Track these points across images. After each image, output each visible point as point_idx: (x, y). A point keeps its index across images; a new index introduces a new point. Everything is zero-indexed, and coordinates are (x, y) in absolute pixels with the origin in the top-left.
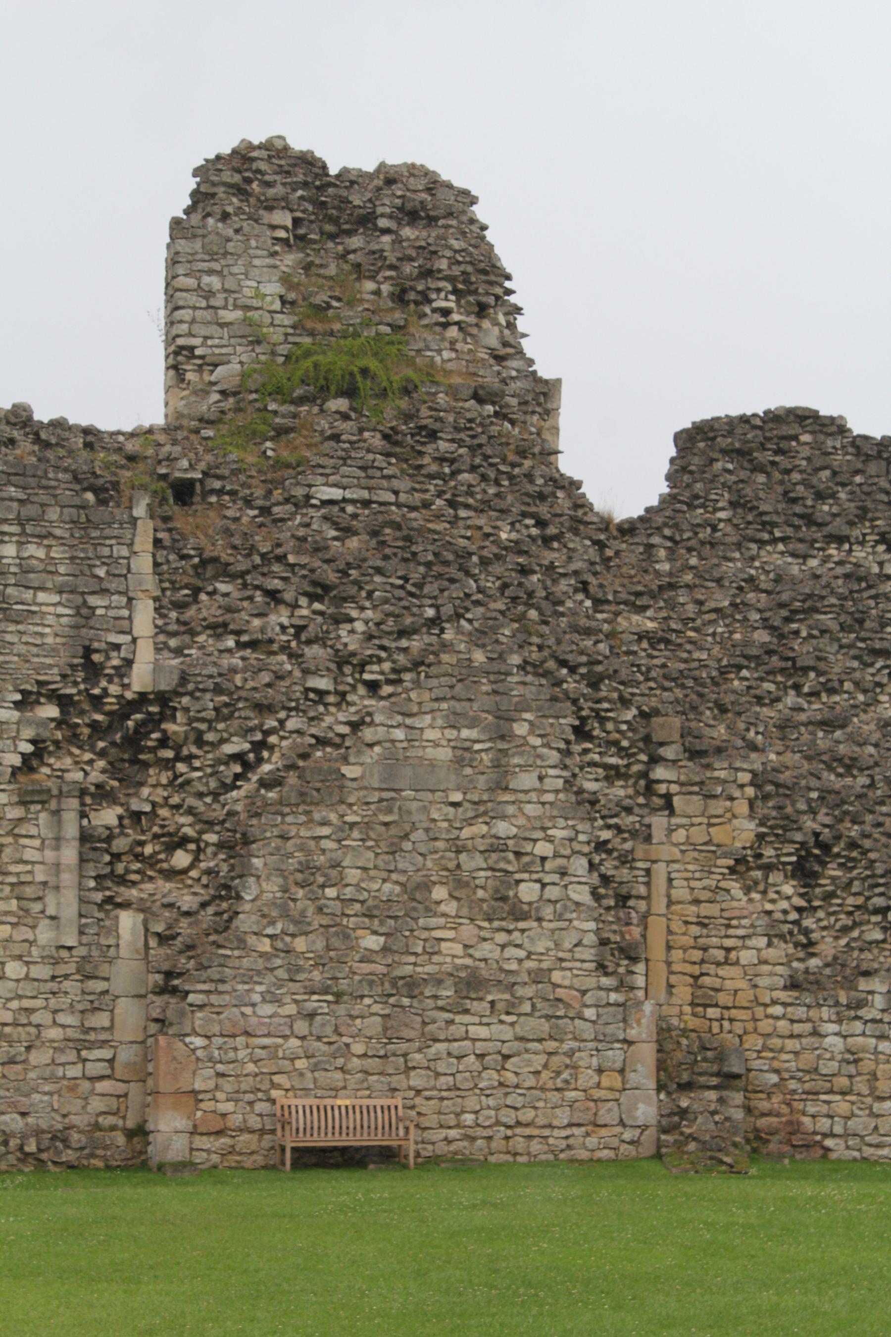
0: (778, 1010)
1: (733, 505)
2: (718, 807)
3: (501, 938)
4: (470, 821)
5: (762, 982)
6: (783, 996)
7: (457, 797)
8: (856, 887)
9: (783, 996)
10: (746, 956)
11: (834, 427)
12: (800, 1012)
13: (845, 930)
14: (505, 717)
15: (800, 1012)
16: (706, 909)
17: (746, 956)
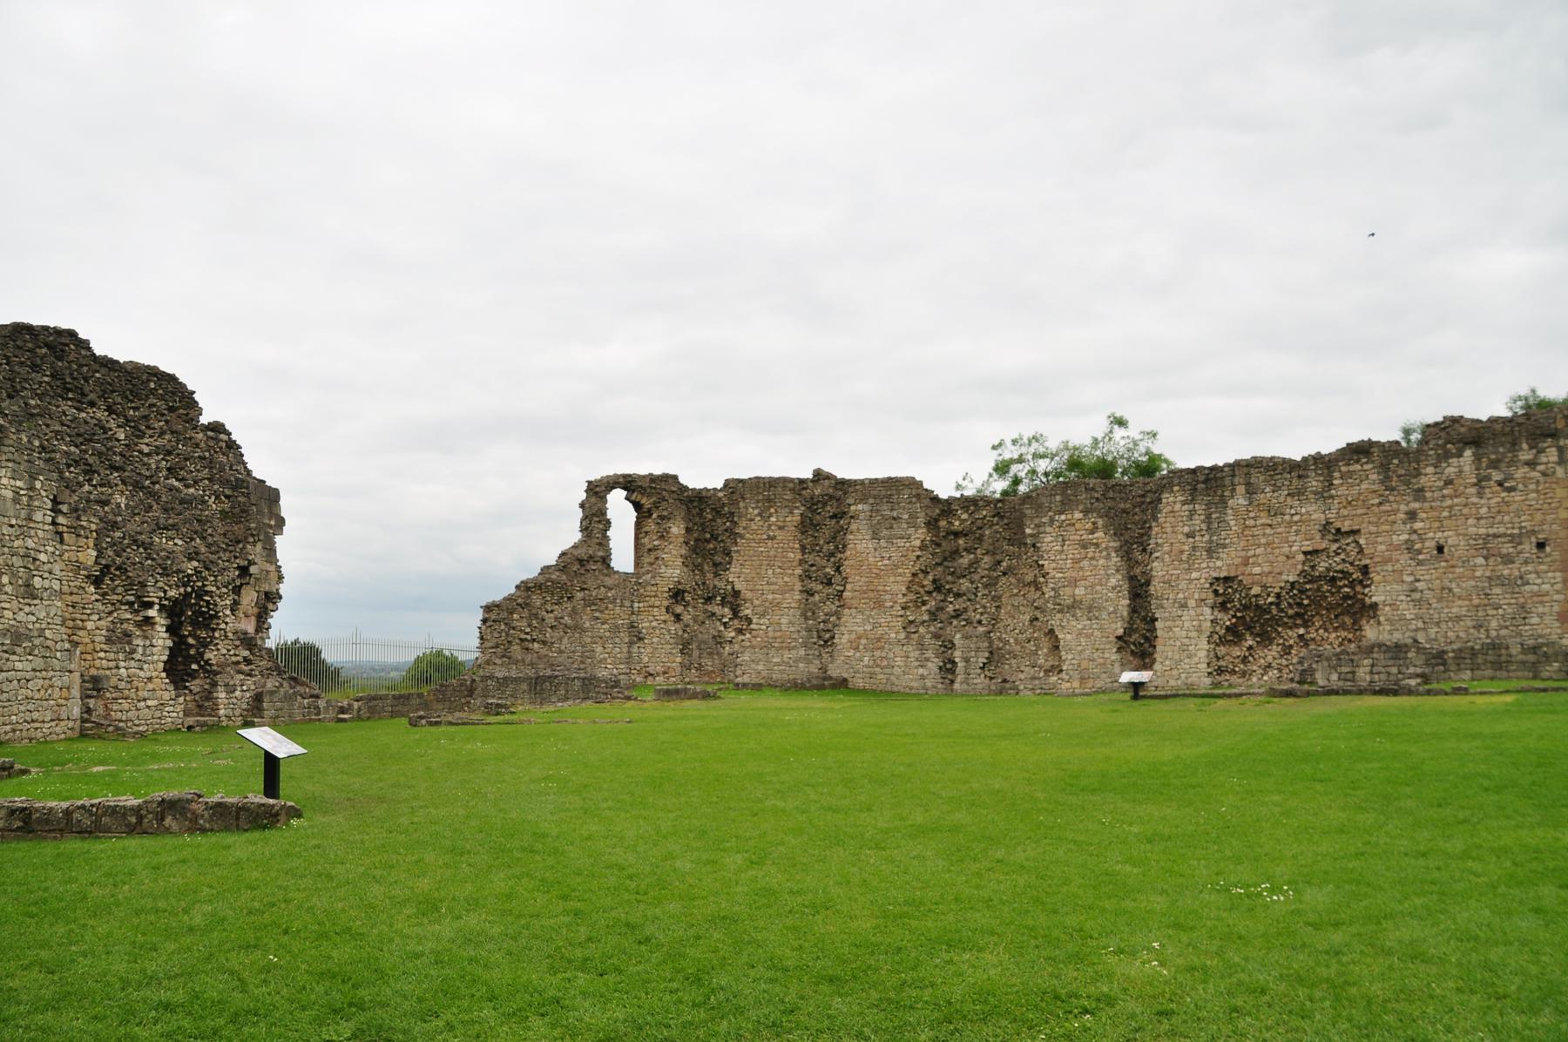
0: (102, 655)
1: (52, 376)
2: (82, 541)
3: (27, 609)
4: (17, 538)
5: (97, 639)
6: (105, 647)
7: (13, 522)
8: (120, 590)
9: (105, 647)
10: (90, 625)
11: (85, 345)
12: (112, 656)
13: (110, 613)
14: (33, 478)
15: (112, 656)
16: (76, 598)
17: (90, 625)
